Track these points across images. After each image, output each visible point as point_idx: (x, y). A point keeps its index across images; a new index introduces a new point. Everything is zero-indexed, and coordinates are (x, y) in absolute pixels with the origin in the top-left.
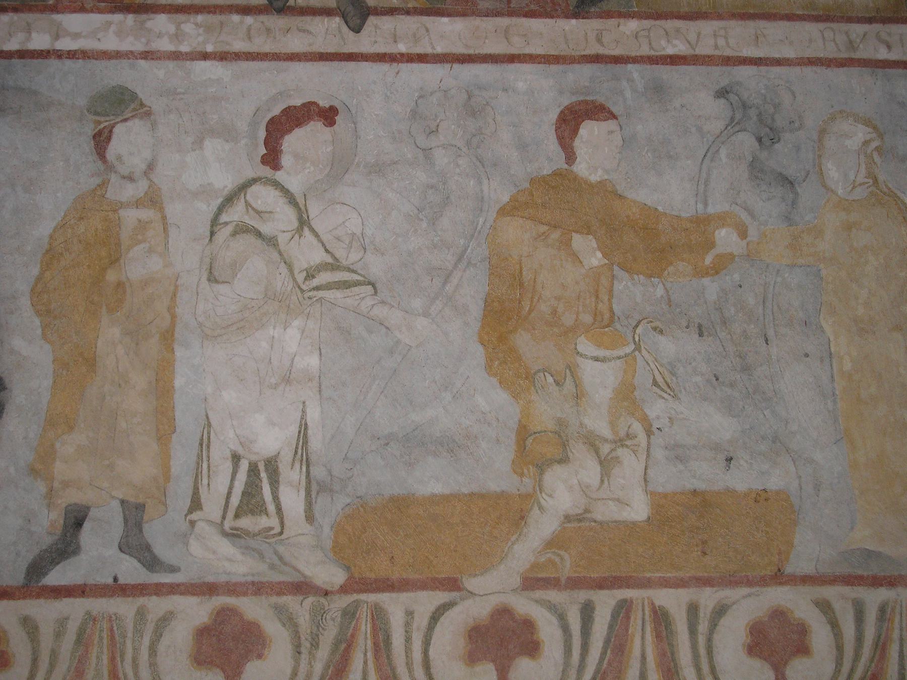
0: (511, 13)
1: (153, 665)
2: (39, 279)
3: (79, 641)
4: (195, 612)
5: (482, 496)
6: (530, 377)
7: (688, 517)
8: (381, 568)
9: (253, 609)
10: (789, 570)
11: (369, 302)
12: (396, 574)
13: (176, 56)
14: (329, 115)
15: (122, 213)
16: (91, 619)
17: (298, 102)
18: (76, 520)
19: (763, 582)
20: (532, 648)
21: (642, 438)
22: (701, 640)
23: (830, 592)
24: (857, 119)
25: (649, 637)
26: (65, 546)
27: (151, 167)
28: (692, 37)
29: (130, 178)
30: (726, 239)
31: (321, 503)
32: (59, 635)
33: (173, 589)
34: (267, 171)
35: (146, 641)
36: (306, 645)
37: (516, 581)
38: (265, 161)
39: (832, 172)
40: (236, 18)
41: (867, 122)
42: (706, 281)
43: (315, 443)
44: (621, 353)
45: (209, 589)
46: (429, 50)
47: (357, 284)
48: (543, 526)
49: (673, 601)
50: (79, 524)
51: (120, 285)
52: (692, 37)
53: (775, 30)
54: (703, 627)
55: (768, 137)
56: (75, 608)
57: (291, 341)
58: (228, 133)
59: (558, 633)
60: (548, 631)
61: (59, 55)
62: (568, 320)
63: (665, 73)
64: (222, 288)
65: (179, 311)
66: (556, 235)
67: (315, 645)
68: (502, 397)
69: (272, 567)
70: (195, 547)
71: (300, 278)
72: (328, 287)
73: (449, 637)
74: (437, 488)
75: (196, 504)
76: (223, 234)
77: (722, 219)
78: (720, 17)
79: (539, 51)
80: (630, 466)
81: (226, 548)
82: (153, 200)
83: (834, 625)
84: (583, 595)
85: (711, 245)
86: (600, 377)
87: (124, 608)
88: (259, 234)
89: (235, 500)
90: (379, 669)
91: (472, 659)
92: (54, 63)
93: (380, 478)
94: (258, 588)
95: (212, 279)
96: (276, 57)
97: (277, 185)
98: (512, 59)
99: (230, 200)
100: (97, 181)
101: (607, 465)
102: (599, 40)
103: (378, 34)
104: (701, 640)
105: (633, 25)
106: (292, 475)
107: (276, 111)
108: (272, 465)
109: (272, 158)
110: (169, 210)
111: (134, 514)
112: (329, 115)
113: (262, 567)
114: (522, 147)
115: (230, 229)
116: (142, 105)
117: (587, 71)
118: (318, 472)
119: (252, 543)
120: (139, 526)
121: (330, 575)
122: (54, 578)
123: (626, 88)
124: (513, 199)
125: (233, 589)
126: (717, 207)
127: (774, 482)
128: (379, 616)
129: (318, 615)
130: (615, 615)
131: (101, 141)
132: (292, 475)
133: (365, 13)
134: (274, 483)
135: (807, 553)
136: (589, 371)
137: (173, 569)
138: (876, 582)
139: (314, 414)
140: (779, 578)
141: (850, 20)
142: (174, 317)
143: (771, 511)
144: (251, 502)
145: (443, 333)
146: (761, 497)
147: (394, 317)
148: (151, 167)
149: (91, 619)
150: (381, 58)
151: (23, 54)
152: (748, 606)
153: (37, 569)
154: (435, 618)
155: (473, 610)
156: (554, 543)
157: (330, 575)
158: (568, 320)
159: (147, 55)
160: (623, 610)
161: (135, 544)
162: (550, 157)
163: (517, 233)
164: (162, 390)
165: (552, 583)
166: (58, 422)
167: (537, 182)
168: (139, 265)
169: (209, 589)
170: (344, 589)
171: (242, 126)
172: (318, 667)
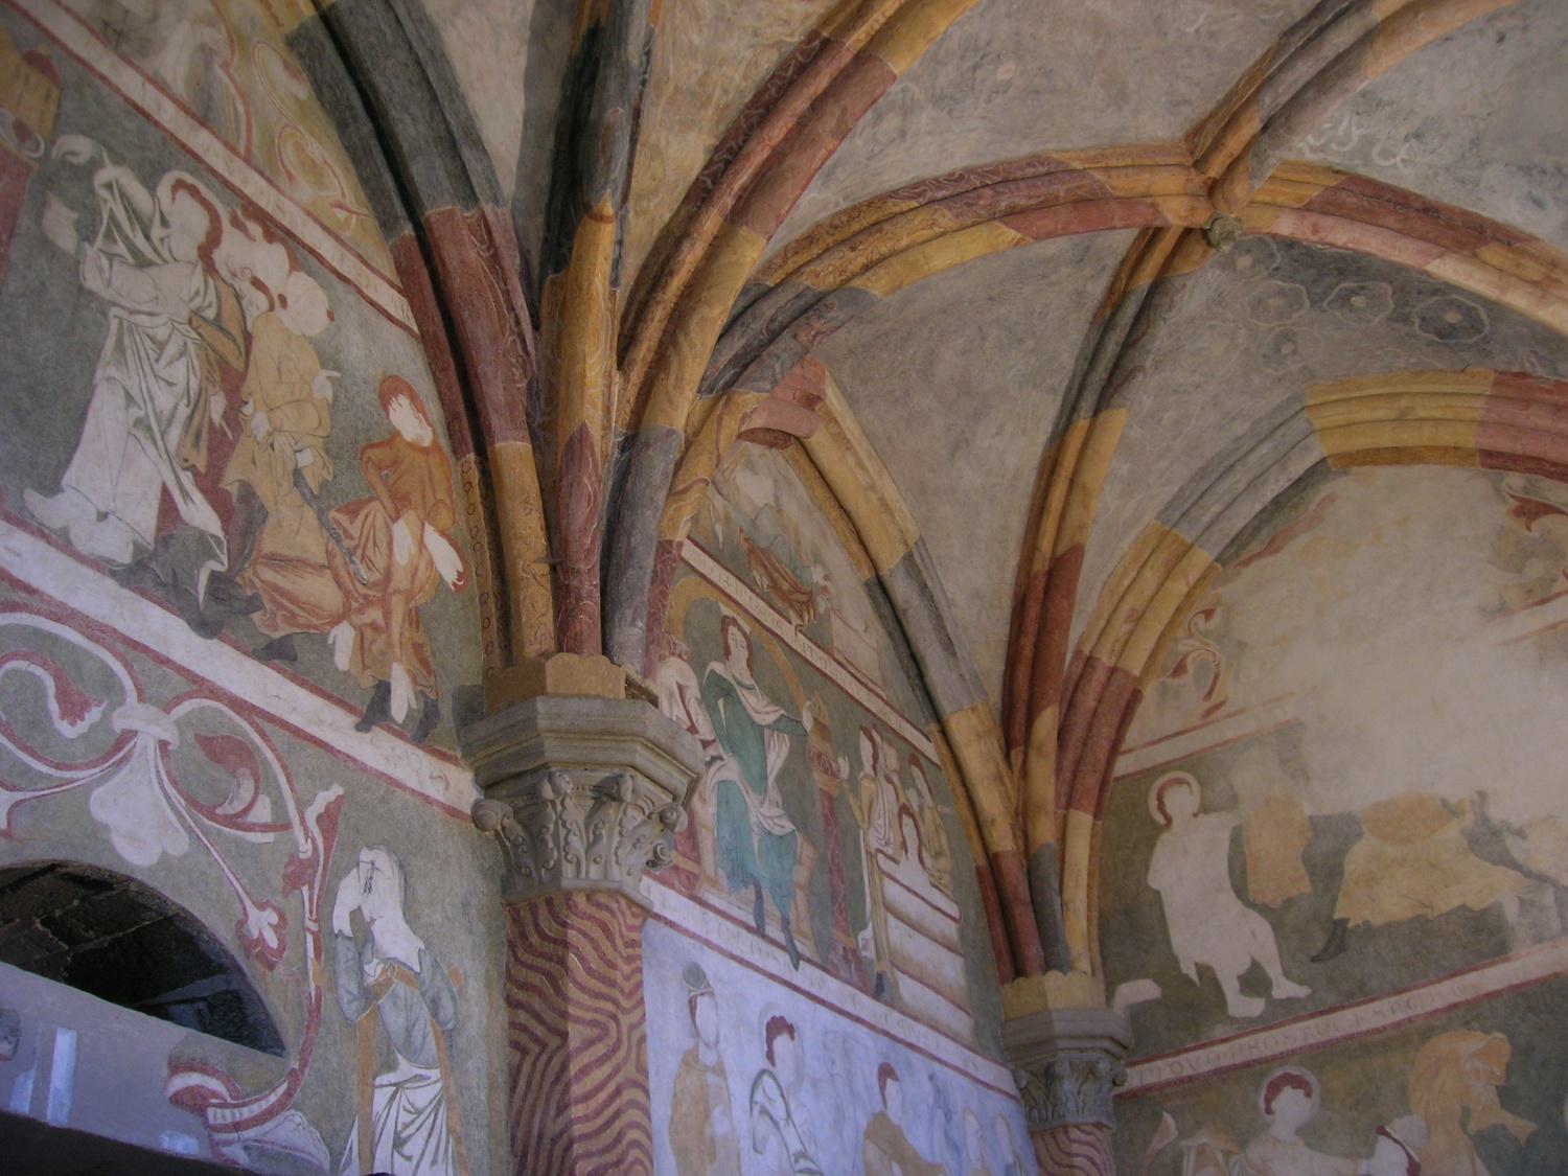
64: (760, 1157)
95: (755, 1149)
98: (858, 1020)
109: (770, 1056)
116: (708, 985)
150: (808, 995)
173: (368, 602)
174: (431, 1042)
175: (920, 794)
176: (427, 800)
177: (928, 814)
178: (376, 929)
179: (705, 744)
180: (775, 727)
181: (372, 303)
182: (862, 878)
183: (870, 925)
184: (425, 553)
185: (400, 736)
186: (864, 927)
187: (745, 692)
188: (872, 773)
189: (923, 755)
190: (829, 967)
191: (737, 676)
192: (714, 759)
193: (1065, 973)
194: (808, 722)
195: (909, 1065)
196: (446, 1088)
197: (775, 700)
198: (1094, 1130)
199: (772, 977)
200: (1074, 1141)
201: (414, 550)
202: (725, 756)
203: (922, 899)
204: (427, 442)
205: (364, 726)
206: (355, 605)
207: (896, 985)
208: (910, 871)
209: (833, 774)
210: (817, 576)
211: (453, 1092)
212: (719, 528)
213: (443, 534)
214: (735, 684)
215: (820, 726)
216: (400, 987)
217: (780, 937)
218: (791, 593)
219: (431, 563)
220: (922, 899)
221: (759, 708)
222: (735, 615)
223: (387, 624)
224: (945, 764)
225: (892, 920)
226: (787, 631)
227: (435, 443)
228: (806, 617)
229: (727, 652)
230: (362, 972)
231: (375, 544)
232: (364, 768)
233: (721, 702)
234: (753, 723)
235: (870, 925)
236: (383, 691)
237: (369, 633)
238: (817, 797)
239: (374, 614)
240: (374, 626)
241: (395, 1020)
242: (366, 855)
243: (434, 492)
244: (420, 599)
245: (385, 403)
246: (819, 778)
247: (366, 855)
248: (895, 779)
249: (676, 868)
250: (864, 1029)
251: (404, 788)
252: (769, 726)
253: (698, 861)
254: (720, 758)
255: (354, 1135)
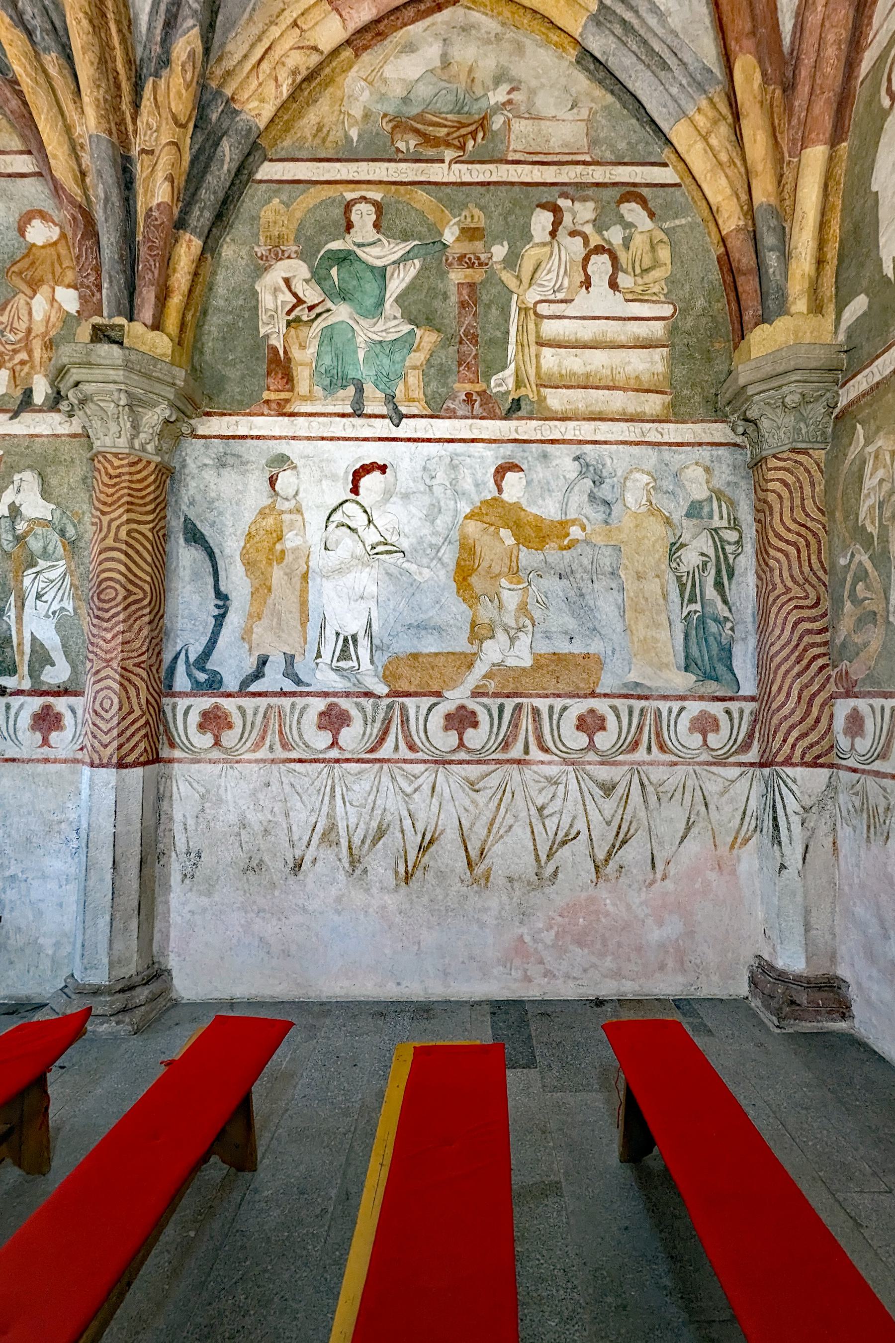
0: (473, 418)
1: (299, 729)
2: (244, 548)
3: (264, 717)
4: (320, 704)
5: (453, 654)
6: (477, 598)
7: (551, 665)
8: (404, 686)
9: (344, 703)
10: (598, 691)
11: (401, 560)
12: (412, 689)
13: (309, 438)
14: (383, 469)
15: (284, 516)
16: (270, 707)
17: (368, 462)
18: (263, 661)
19: (585, 696)
20: (475, 725)
21: (530, 628)
22: (555, 722)
23: (617, 702)
24: (643, 472)
25: (530, 720)
26: (258, 674)
27: (297, 494)
28: (563, 430)
29: (287, 499)
30: (575, 532)
31: (377, 655)
32: (255, 714)
33: (308, 694)
34: (353, 496)
35: (296, 718)
36: (369, 720)
37: (469, 693)
38: (352, 491)
39: (630, 499)
40: (338, 419)
41: (648, 474)
42: (564, 552)
43: (375, 627)
44: (521, 586)
45: (326, 695)
46: (432, 437)
47: (396, 552)
48: (481, 668)
49: (542, 704)
50: (264, 663)
51: (283, 552)
52: (563, 430)
53: (604, 426)
54: (555, 717)
55: (598, 482)
56: (263, 702)
57: (365, 579)
58: (334, 477)
59: (487, 718)
60: (483, 717)
61: (252, 437)
62: (496, 569)
63: (549, 448)
65: (311, 564)
66: (493, 528)
67: (374, 721)
68: (464, 606)
69: (354, 685)
70: (319, 675)
71: (369, 548)
72: (381, 553)
73: (436, 720)
74: (433, 650)
75: (319, 655)
76: (332, 526)
77: (574, 522)
78: (577, 420)
79: (487, 437)
80: (524, 640)
81: (333, 676)
82: (299, 511)
83: (618, 717)
84: (499, 701)
85: (568, 534)
86: (511, 599)
87: (286, 702)
88: (349, 528)
89: (337, 654)
90: (403, 732)
91: (446, 729)
92: (249, 441)
93: (404, 645)
94: (347, 695)
95: (326, 548)
96: (357, 439)
97: (357, 503)
98: (473, 441)
99: (335, 510)
100: (271, 500)
101: (512, 640)
102: (516, 431)
103: (408, 428)
104: (555, 722)
105: (534, 423)
106: (364, 642)
107: (358, 467)
108: (354, 638)
109: (355, 490)
110: (307, 515)
111: (290, 660)
112: (383, 469)
113: (349, 685)
114: (477, 485)
115: (335, 524)
117: (510, 446)
118: (376, 641)
119: (345, 673)
120: (292, 664)
121: (382, 689)
122: (253, 688)
123: (527, 456)
124: (472, 511)
125: (335, 694)
126: (572, 515)
127: (592, 650)
128: (403, 708)
129: (376, 707)
130: (514, 710)
131: (272, 481)
132: (364, 642)
133: (402, 416)
134: (355, 646)
135: (607, 683)
136: (505, 595)
137: (308, 685)
138: (640, 697)
139: (374, 615)
140: (593, 694)
141: (643, 421)
142: (308, 567)
143: (590, 664)
144: (344, 655)
145: (436, 576)
146: (586, 656)
147: (413, 568)
148: (297, 494)
149: (270, 707)
150: (409, 440)
151: (234, 437)
152: (578, 707)
153: (245, 684)
154: (430, 710)
155: (446, 707)
156: (488, 676)
157: (382, 689)
158: (496, 569)
159: (294, 438)
160: (518, 707)
161: (290, 673)
162: (490, 491)
163: (473, 528)
164: (304, 603)
165: (485, 694)
166: (255, 616)
167: (484, 502)
168: (291, 540)
169: (326, 695)
170: (388, 696)
171: (341, 473)
172: (375, 731)
173: (15, 351)
174: (60, 550)
175: (628, 225)
176: (57, 436)
177: (639, 241)
178: (22, 509)
179: (311, 308)
180: (405, 258)
181: (10, 176)
182: (508, 333)
183: (512, 366)
184: (55, 304)
185: (41, 411)
186: (505, 367)
187: (367, 249)
188: (548, 238)
189: (648, 185)
190: (442, 413)
191: (359, 240)
192: (318, 315)
193: (771, 324)
194: (450, 235)
195: (545, 456)
196: (69, 567)
197: (405, 237)
198: (791, 455)
199: (365, 439)
200: (771, 469)
201: (47, 307)
202: (333, 307)
203: (607, 318)
204: (55, 238)
205: (15, 415)
206: (7, 358)
207: (542, 399)
208: (600, 299)
209: (480, 264)
210: (499, 96)
211: (73, 568)
212: (354, 133)
213: (69, 286)
214: (355, 249)
215: (470, 233)
216: (39, 530)
217: (384, 410)
218: (448, 134)
219: (60, 306)
220: (607, 318)
221: (383, 253)
222: (363, 193)
223: (30, 357)
224: (682, 179)
225: (546, 352)
226: (437, 173)
227: (63, 236)
228: (470, 144)
229: (349, 226)
230: (14, 529)
231: (19, 318)
232: (16, 436)
233: (334, 271)
234: (372, 268)
235: (512, 366)
236: (28, 393)
237: (18, 368)
238: (453, 290)
239: (23, 356)
240: (23, 363)
241: (35, 545)
242: (17, 477)
243: (61, 265)
244: (52, 333)
245: (22, 232)
246: (457, 276)
247: (17, 477)
248: (588, 229)
249: (267, 402)
250: (481, 445)
251: (41, 436)
252: (394, 263)
253: (292, 390)
254: (328, 310)
255: (12, 598)
